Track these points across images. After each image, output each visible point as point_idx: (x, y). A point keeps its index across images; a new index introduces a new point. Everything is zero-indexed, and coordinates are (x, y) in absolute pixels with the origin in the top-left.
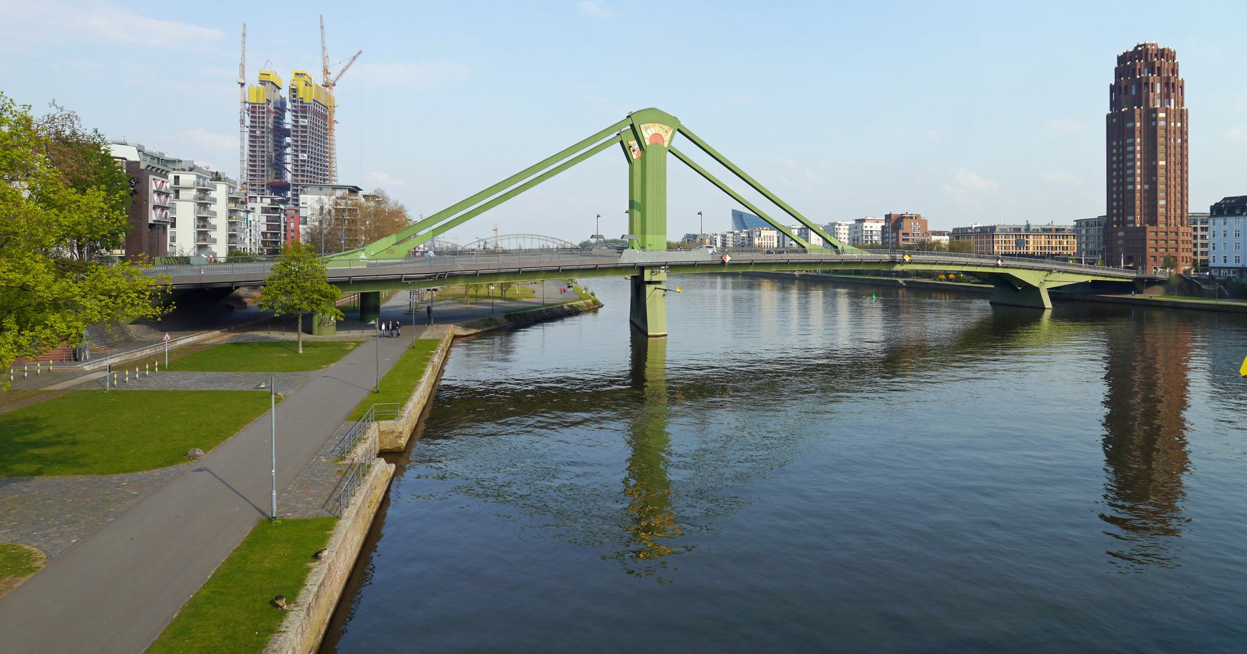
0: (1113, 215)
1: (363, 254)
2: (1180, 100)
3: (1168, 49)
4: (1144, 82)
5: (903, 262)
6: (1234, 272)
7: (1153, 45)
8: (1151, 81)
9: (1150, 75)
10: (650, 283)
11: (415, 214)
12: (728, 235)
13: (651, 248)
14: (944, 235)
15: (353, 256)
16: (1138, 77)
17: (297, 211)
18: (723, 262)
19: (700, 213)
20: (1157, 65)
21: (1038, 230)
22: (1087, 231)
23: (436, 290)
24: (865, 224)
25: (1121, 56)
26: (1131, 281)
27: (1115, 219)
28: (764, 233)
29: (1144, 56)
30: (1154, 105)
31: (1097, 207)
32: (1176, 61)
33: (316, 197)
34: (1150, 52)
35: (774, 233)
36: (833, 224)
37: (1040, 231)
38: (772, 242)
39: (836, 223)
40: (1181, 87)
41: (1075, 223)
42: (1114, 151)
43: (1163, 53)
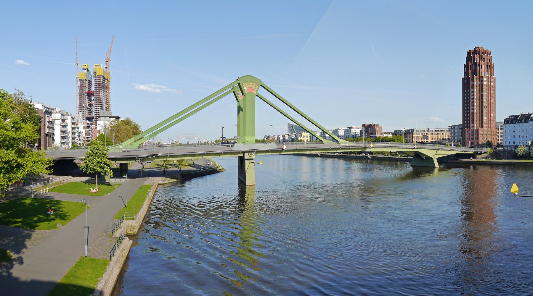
0: (465, 124)
1: (121, 146)
2: (492, 73)
3: (488, 50)
4: (478, 64)
5: (370, 147)
6: (513, 148)
7: (482, 48)
8: (481, 64)
9: (480, 61)
10: (247, 159)
11: (143, 128)
12: (286, 136)
13: (248, 143)
14: (390, 134)
15: (117, 147)
16: (476, 62)
17: (96, 128)
18: (283, 149)
19: (271, 126)
20: (483, 57)
21: (433, 131)
22: (454, 131)
23: (150, 163)
24: (352, 129)
25: (469, 52)
26: (473, 153)
27: (466, 125)
28: (303, 134)
29: (478, 53)
30: (482, 75)
31: (459, 121)
32: (491, 56)
33: (103, 122)
34: (480, 51)
35: (308, 134)
36: (337, 130)
37: (434, 131)
38: (307, 139)
39: (338, 129)
40: (493, 67)
41: (449, 127)
42: (466, 95)
43: (486, 52)
